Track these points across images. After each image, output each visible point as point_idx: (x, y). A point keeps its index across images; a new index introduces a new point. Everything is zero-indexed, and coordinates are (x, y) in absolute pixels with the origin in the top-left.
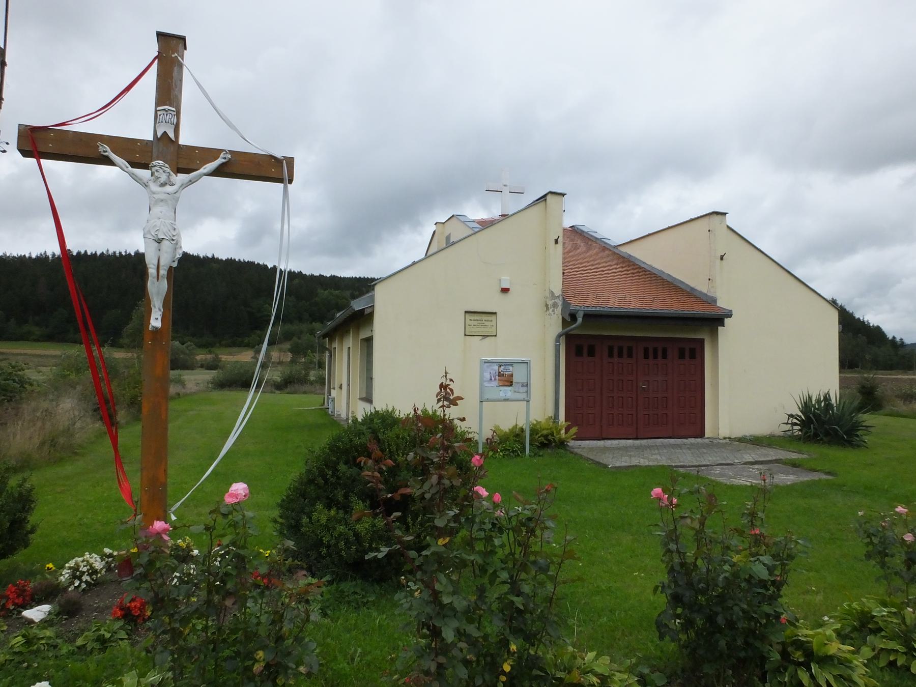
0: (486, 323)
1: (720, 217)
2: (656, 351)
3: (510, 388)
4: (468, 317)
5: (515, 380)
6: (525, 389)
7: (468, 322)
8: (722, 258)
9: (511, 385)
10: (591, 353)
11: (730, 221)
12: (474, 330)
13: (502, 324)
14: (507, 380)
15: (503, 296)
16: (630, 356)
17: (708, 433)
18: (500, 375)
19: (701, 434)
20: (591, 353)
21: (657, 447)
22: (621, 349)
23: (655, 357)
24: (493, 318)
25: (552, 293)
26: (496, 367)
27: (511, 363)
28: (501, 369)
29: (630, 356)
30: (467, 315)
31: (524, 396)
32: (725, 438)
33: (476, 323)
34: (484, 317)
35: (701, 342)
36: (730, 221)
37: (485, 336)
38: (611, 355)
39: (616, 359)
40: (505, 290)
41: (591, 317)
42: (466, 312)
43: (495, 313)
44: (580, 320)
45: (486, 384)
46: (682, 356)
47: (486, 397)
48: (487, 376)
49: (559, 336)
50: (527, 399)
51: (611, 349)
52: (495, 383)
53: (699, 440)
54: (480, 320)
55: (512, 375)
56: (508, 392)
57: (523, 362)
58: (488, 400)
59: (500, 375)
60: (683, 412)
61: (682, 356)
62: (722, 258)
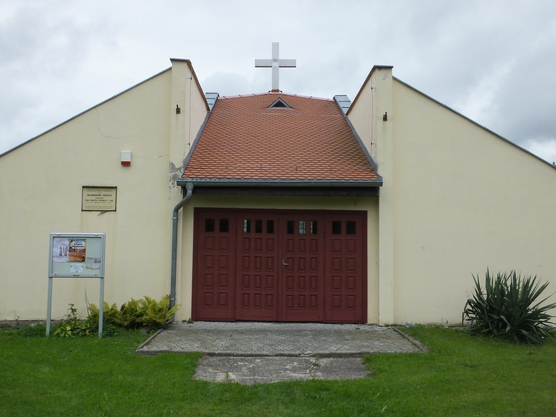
0: (105, 198)
1: (388, 71)
3: (80, 265)
4: (86, 192)
5: (87, 255)
6: (98, 265)
7: (86, 197)
8: (385, 118)
9: (83, 261)
11: (395, 73)
12: (93, 205)
13: (123, 198)
15: (126, 170)
16: (270, 230)
17: (371, 318)
19: (363, 320)
20: (224, 227)
21: (328, 333)
24: (113, 192)
25: (172, 165)
26: (67, 242)
27: (84, 239)
28: (73, 244)
29: (270, 230)
30: (85, 190)
31: (97, 272)
32: (387, 326)
33: (93, 198)
34: (103, 192)
35: (363, 215)
36: (395, 73)
40: (126, 164)
41: (199, 189)
42: (83, 187)
43: (116, 188)
44: (189, 192)
45: (55, 260)
46: (336, 228)
47: (56, 272)
48: (57, 251)
49: (176, 210)
50: (100, 275)
52: (65, 259)
53: (362, 327)
54: (99, 195)
55: (84, 251)
56: (79, 268)
58: (56, 276)
60: (343, 294)
62: (385, 118)
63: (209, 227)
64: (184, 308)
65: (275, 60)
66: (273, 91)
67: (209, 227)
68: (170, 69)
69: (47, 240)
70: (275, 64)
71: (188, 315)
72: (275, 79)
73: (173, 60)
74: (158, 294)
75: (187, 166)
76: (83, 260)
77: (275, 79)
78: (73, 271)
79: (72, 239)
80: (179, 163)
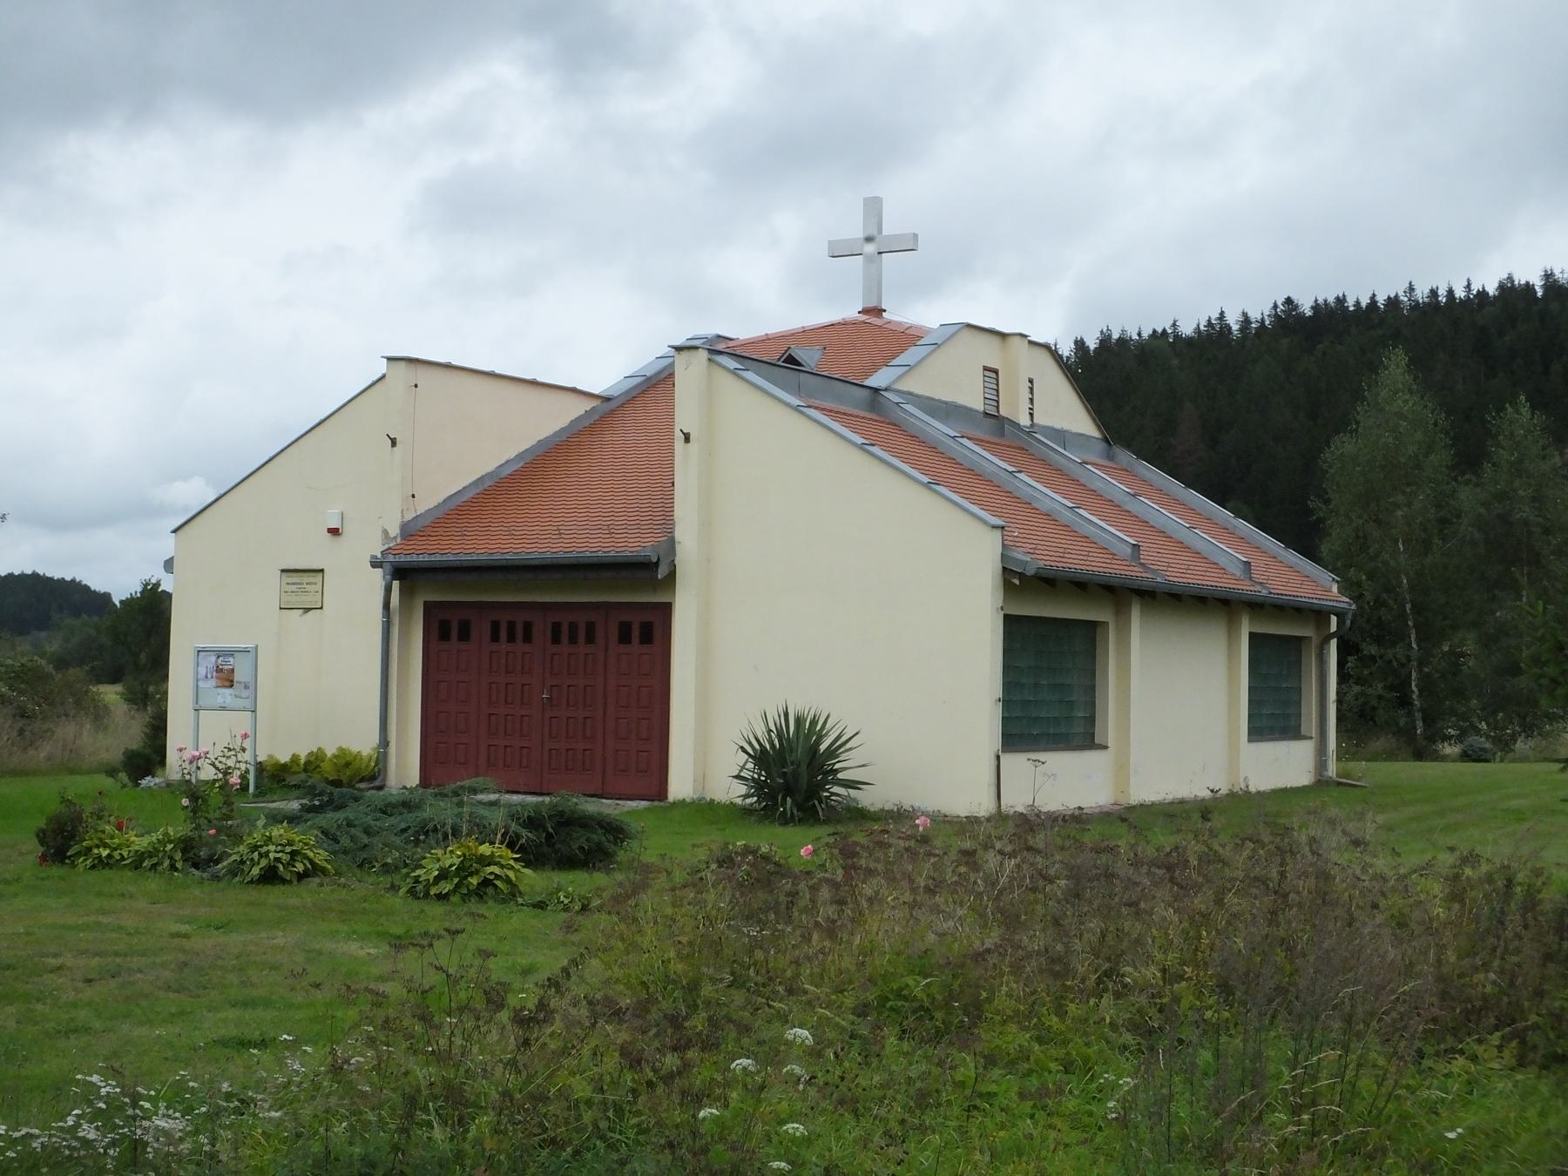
0: (309, 588)
2: (570, 629)
3: (228, 691)
10: (464, 635)
14: (227, 679)
18: (219, 670)
20: (464, 635)
22: (512, 627)
23: (573, 639)
25: (385, 532)
27: (231, 653)
33: (294, 588)
34: (306, 578)
37: (307, 610)
38: (495, 637)
39: (504, 646)
40: (334, 532)
43: (322, 571)
45: (201, 684)
46: (625, 638)
48: (202, 671)
51: (495, 626)
52: (213, 683)
56: (226, 695)
57: (246, 651)
59: (219, 670)
61: (625, 638)
63: (444, 635)
64: (406, 769)
65: (869, 239)
66: (865, 311)
67: (444, 635)
68: (384, 376)
69: (193, 654)
70: (870, 248)
71: (413, 777)
72: (874, 282)
73: (389, 359)
74: (363, 743)
75: (409, 532)
76: (230, 683)
77: (874, 282)
78: (220, 700)
79: (220, 653)
80: (394, 531)
